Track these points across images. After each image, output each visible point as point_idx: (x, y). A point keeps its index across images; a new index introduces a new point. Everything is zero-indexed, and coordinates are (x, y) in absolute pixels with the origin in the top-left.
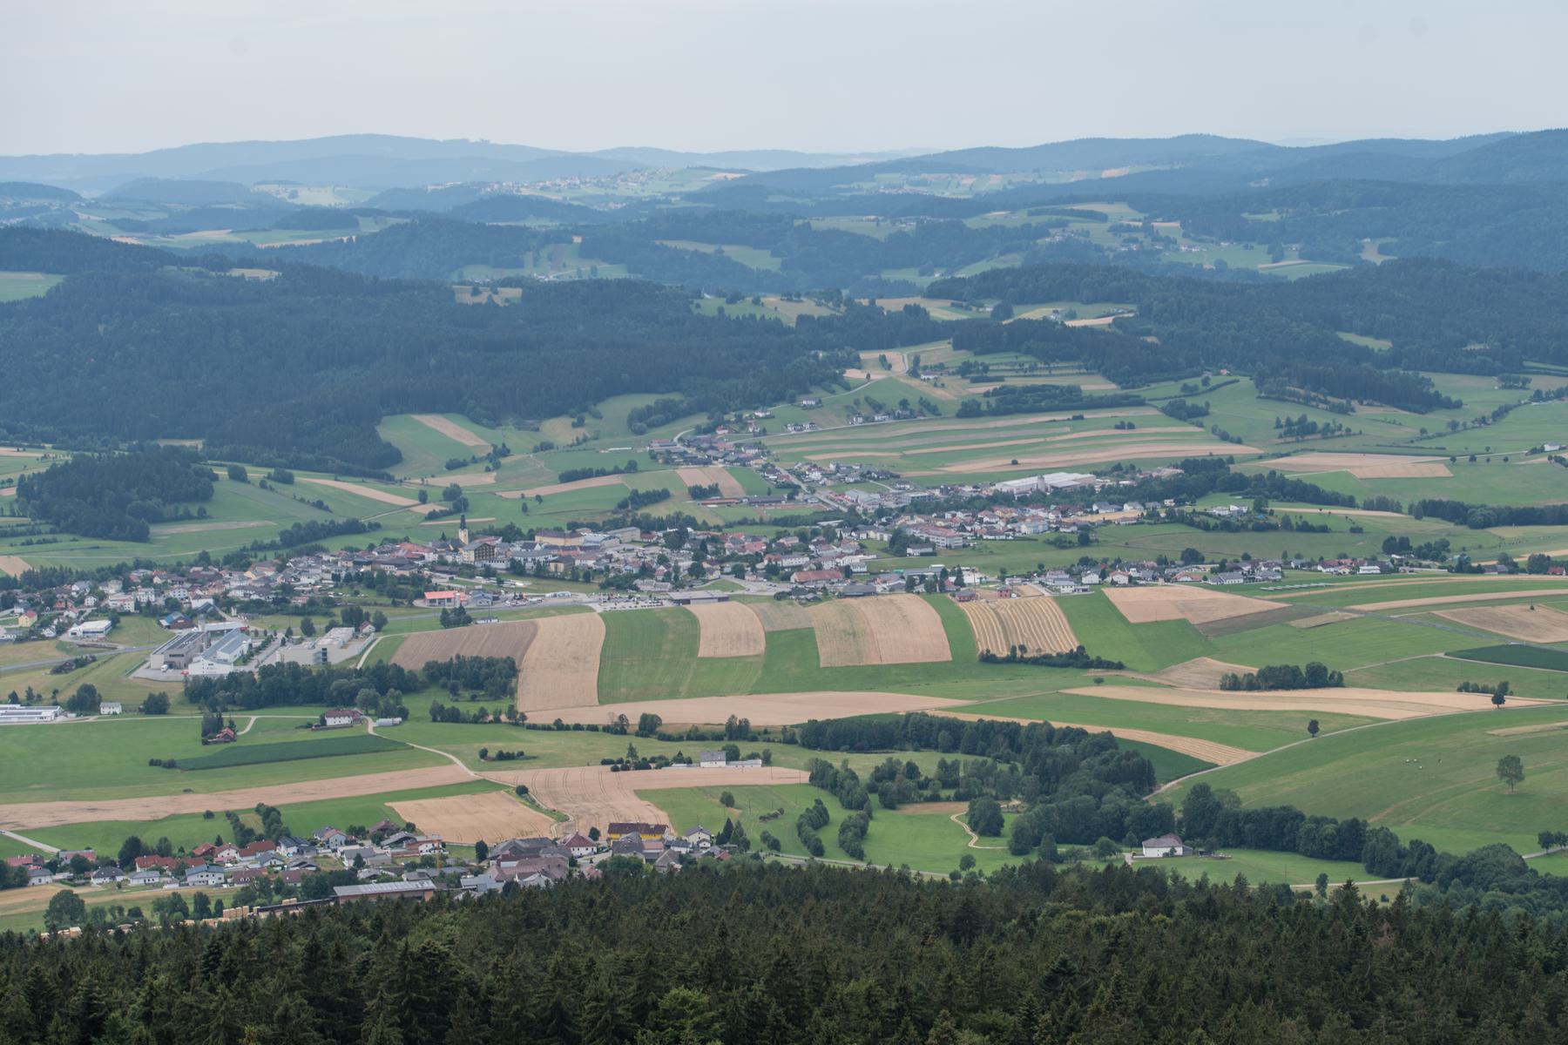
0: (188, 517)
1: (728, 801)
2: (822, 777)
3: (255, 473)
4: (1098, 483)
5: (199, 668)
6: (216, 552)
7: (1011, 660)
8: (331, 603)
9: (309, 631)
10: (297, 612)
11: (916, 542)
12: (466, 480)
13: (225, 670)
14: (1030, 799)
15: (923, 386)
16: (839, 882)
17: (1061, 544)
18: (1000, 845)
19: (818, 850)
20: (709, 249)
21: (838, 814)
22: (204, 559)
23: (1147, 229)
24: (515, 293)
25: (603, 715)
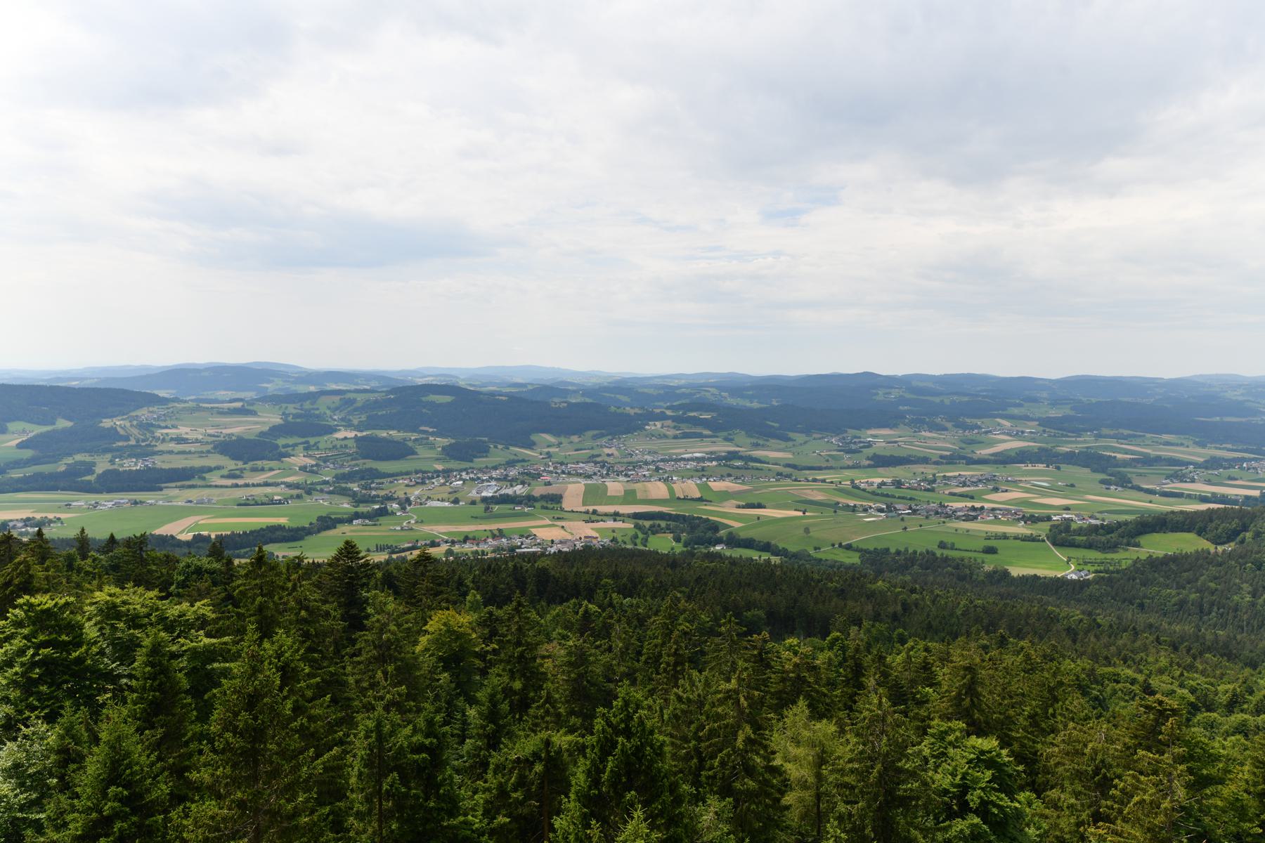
0: (483, 457)
1: (614, 531)
2: (637, 526)
3: (500, 447)
4: (707, 456)
5: (484, 494)
6: (490, 465)
7: (684, 499)
8: (517, 479)
9: (512, 486)
10: (509, 481)
11: (662, 469)
12: (551, 450)
13: (491, 495)
14: (688, 533)
15: (664, 431)
16: (642, 553)
17: (697, 471)
18: (680, 545)
19: (636, 545)
20: (613, 396)
21: (641, 535)
22: (487, 467)
23: (720, 395)
24: (565, 405)
25: (583, 509)
